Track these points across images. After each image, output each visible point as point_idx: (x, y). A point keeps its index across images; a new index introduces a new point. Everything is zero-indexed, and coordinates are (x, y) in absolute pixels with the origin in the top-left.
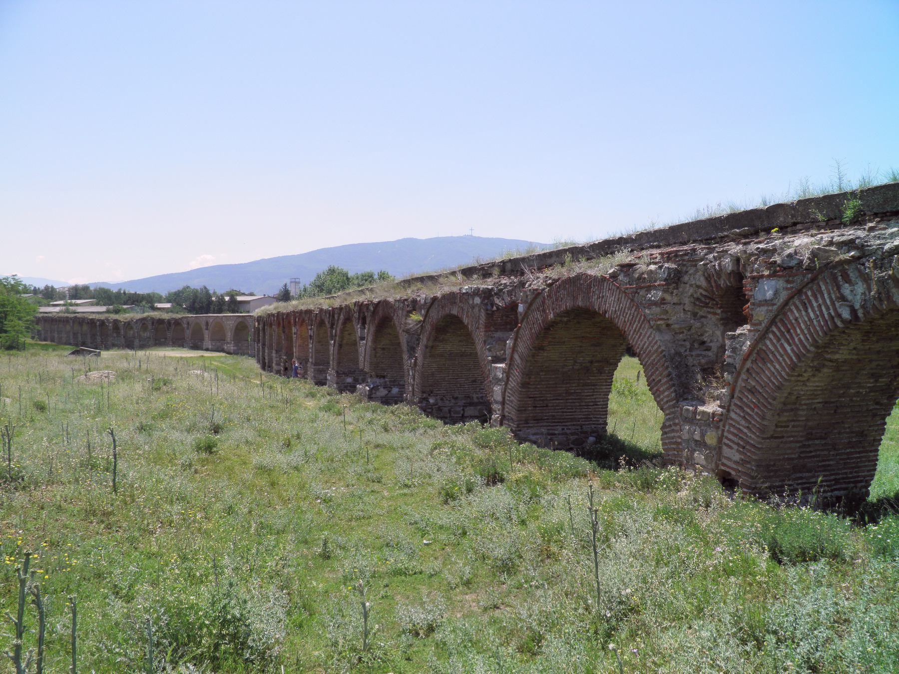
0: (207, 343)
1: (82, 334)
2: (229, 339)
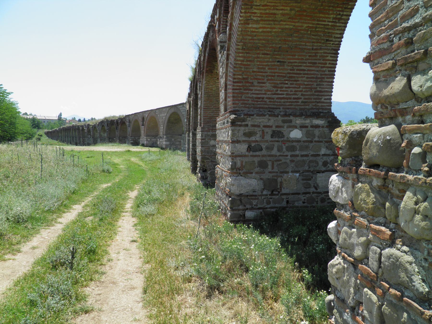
0: (143, 139)
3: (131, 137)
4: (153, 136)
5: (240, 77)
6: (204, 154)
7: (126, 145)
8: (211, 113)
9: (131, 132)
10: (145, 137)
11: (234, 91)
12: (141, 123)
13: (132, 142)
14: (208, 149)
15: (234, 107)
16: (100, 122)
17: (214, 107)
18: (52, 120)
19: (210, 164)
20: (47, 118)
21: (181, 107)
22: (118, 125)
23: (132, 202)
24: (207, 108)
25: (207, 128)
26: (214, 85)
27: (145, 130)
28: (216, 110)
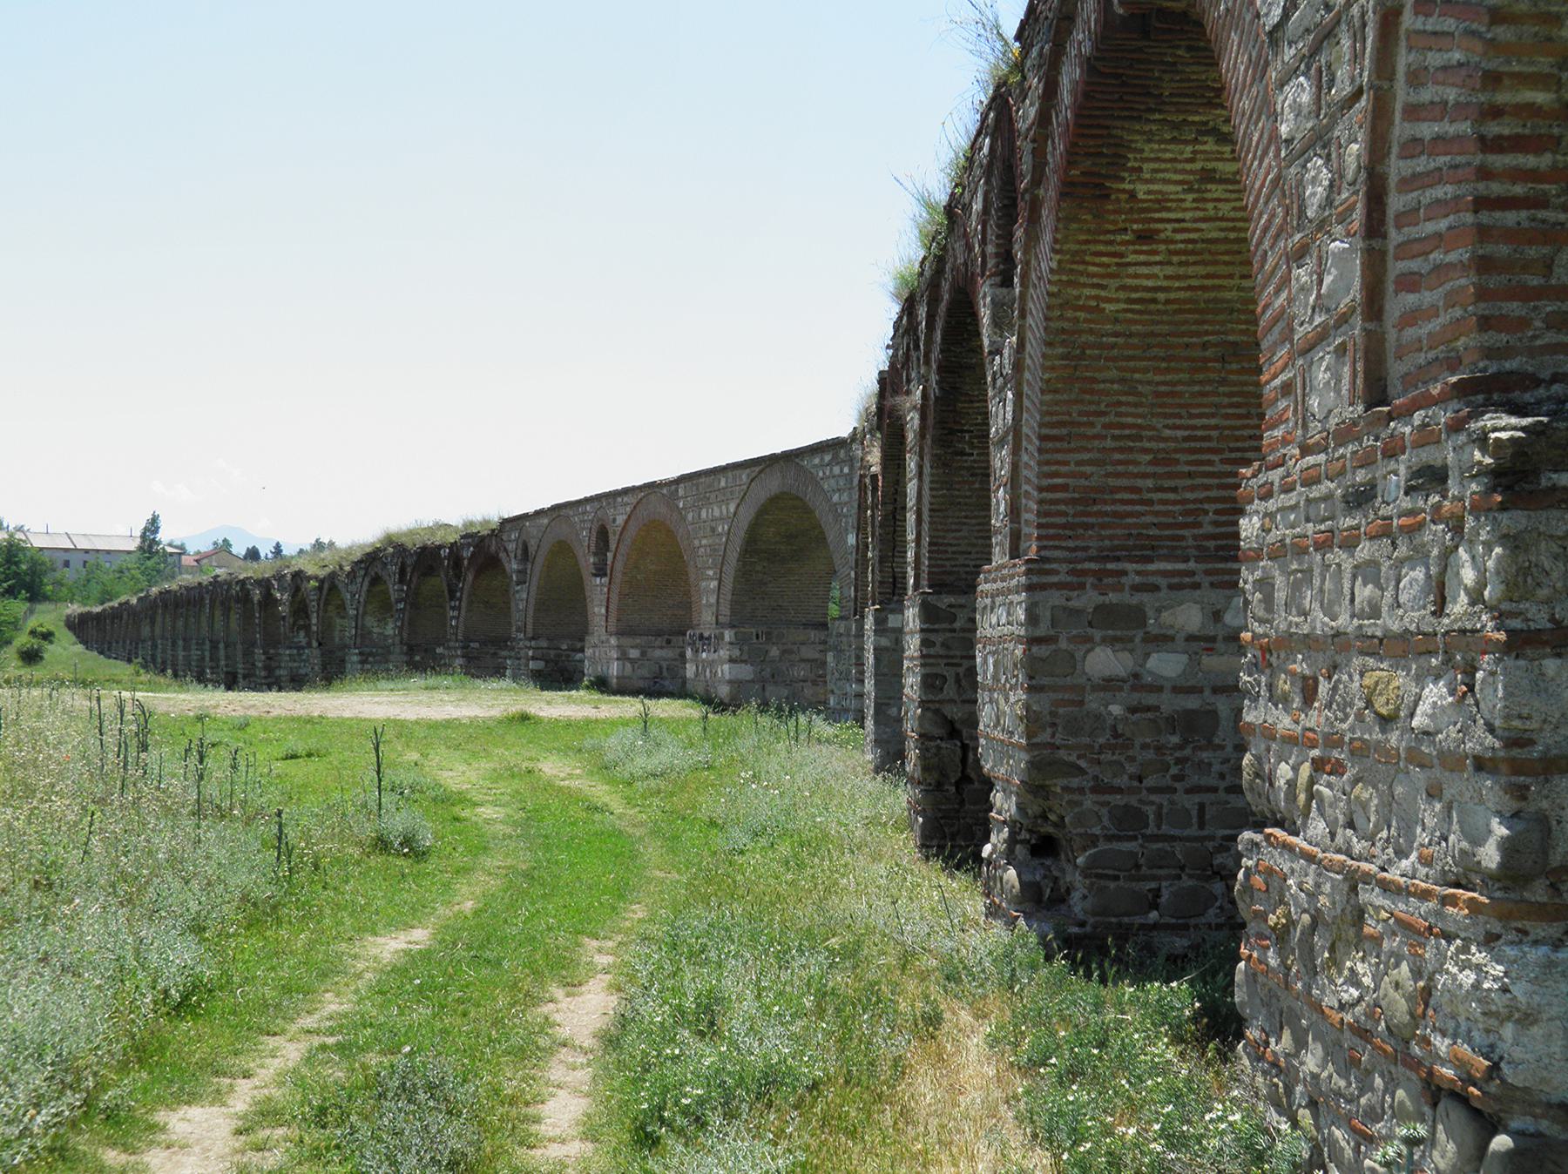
1: (226, 647)
2: (707, 617)
3: (533, 638)
4: (659, 634)
5: (1541, 97)
6: (1045, 737)
7: (506, 683)
8: (1088, 469)
9: (531, 613)
10: (613, 641)
11: (1485, 217)
12: (588, 561)
13: (540, 665)
14: (1073, 703)
15: (1490, 353)
16: (361, 561)
17: (1104, 426)
18: (108, 552)
19: (1089, 802)
20: (83, 544)
21: (822, 466)
22: (458, 576)
23: (579, 1074)
24: (1064, 431)
25: (1064, 567)
26: (1114, 283)
27: (615, 598)
28: (1121, 450)
